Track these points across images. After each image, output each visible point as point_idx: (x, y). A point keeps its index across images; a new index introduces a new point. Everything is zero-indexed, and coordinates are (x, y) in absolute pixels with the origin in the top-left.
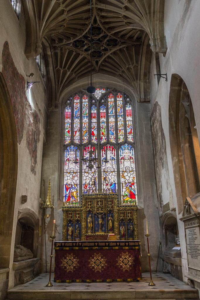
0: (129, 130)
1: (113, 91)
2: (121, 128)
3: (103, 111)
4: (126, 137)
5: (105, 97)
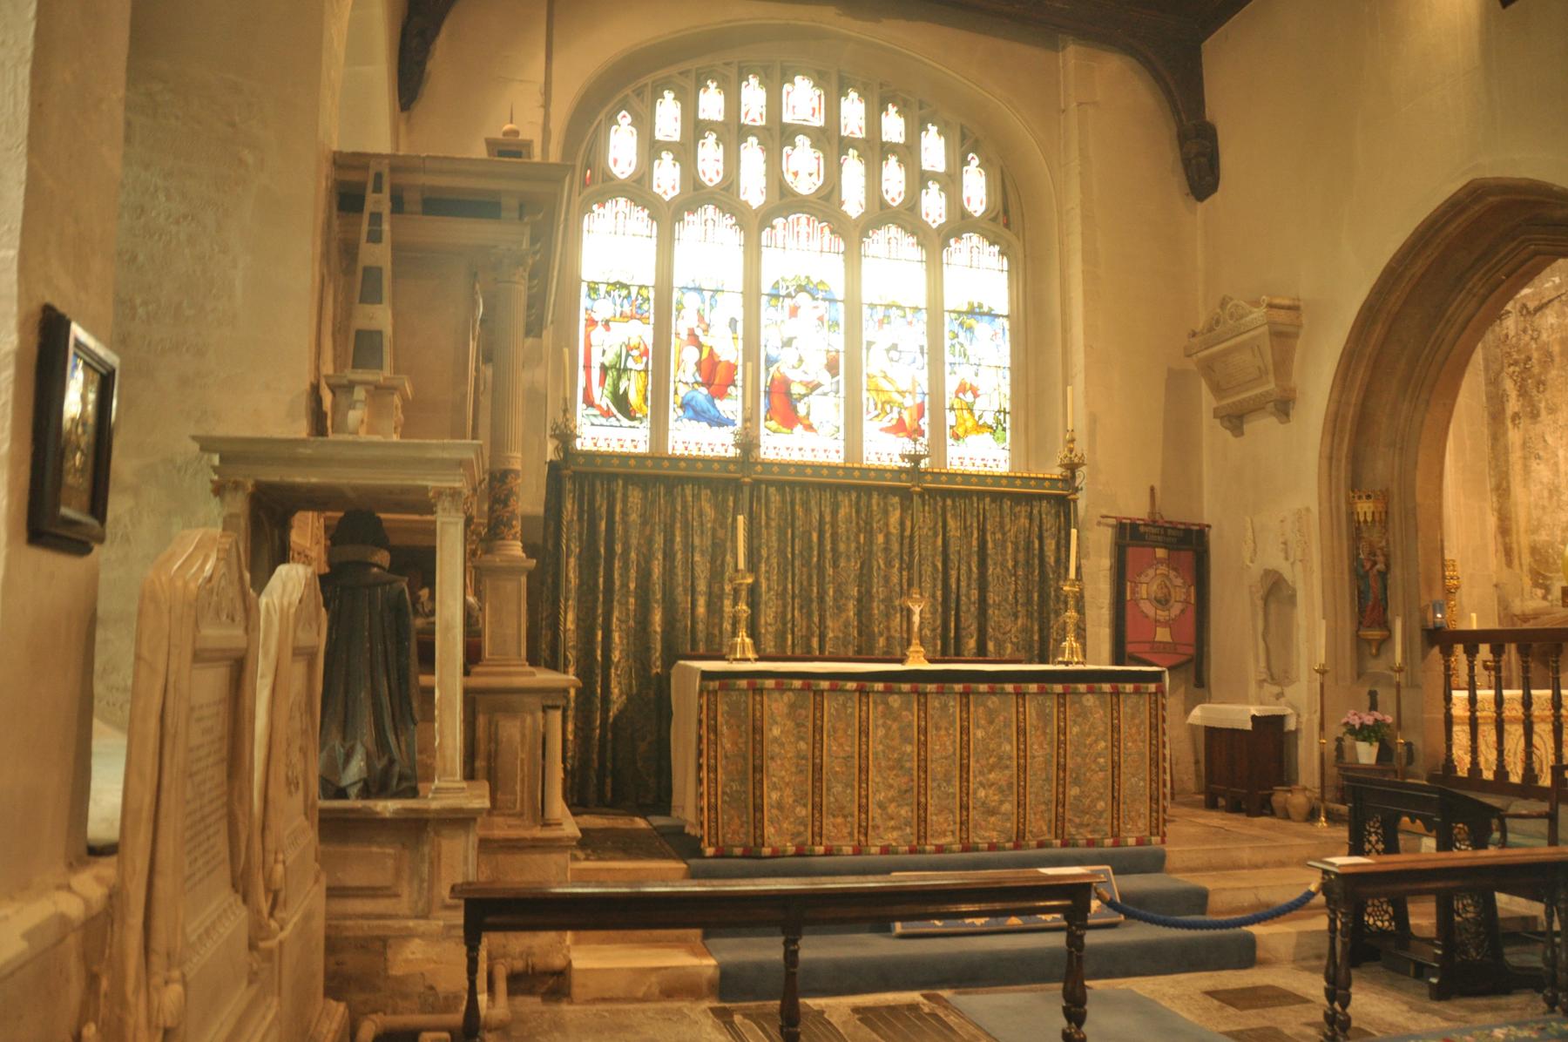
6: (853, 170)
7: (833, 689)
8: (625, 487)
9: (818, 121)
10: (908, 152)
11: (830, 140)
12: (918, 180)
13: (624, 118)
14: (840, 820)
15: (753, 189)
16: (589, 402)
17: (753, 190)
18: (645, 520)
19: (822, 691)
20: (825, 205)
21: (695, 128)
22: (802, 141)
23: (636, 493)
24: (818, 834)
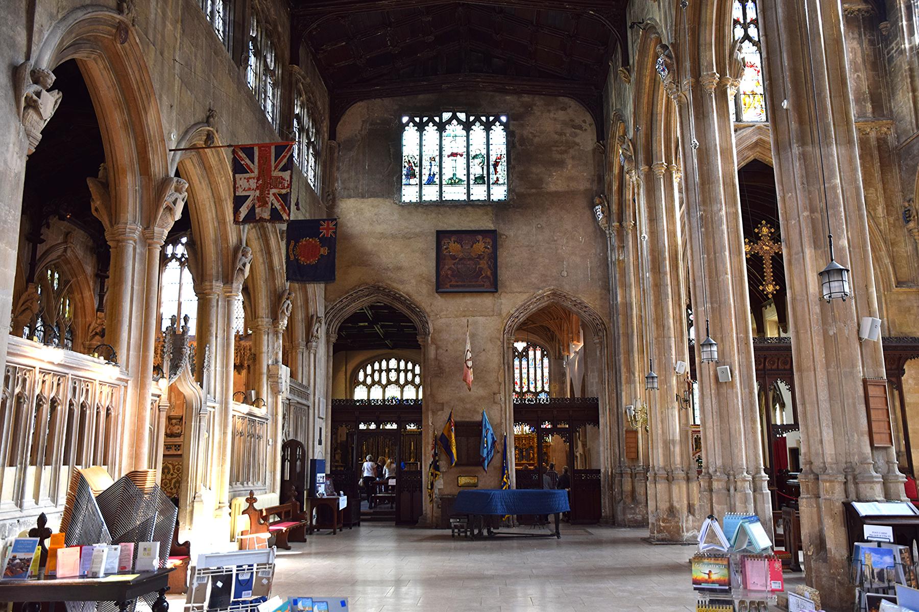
0: (545, 380)
1: (532, 345)
2: (539, 377)
3: (524, 363)
4: (543, 387)
5: (526, 350)
6: (402, 375)
9: (396, 367)
10: (413, 371)
11: (398, 371)
12: (414, 376)
13: (362, 370)
15: (384, 382)
17: (384, 382)
20: (397, 382)
21: (373, 371)
22: (393, 371)
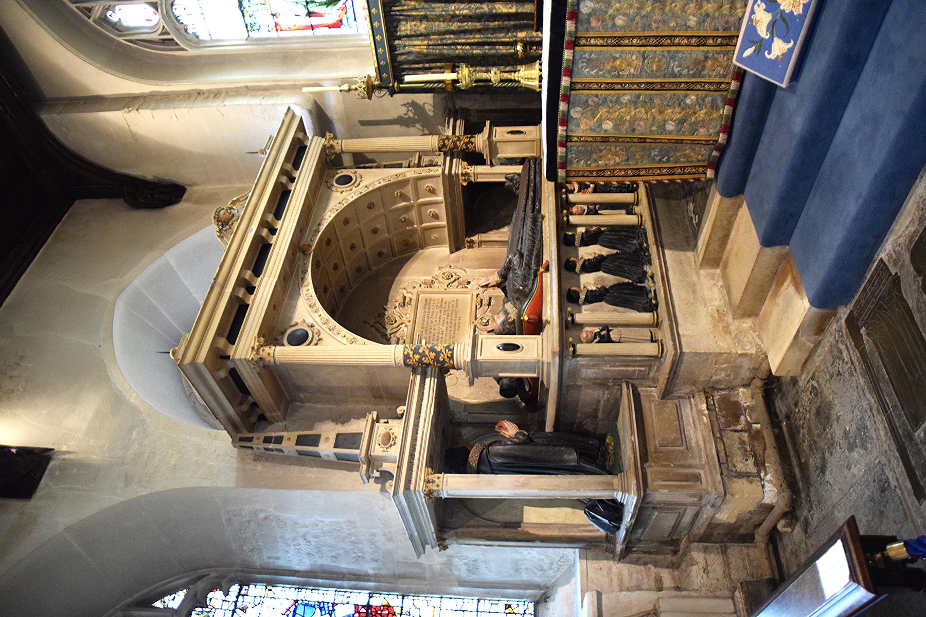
7: (570, 73)
8: (399, 38)
14: (709, 62)
16: (338, 25)
18: (425, 18)
19: (571, 83)
23: (403, 28)
24: (718, 87)
